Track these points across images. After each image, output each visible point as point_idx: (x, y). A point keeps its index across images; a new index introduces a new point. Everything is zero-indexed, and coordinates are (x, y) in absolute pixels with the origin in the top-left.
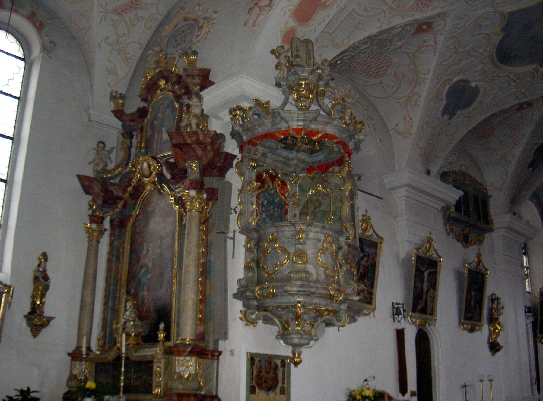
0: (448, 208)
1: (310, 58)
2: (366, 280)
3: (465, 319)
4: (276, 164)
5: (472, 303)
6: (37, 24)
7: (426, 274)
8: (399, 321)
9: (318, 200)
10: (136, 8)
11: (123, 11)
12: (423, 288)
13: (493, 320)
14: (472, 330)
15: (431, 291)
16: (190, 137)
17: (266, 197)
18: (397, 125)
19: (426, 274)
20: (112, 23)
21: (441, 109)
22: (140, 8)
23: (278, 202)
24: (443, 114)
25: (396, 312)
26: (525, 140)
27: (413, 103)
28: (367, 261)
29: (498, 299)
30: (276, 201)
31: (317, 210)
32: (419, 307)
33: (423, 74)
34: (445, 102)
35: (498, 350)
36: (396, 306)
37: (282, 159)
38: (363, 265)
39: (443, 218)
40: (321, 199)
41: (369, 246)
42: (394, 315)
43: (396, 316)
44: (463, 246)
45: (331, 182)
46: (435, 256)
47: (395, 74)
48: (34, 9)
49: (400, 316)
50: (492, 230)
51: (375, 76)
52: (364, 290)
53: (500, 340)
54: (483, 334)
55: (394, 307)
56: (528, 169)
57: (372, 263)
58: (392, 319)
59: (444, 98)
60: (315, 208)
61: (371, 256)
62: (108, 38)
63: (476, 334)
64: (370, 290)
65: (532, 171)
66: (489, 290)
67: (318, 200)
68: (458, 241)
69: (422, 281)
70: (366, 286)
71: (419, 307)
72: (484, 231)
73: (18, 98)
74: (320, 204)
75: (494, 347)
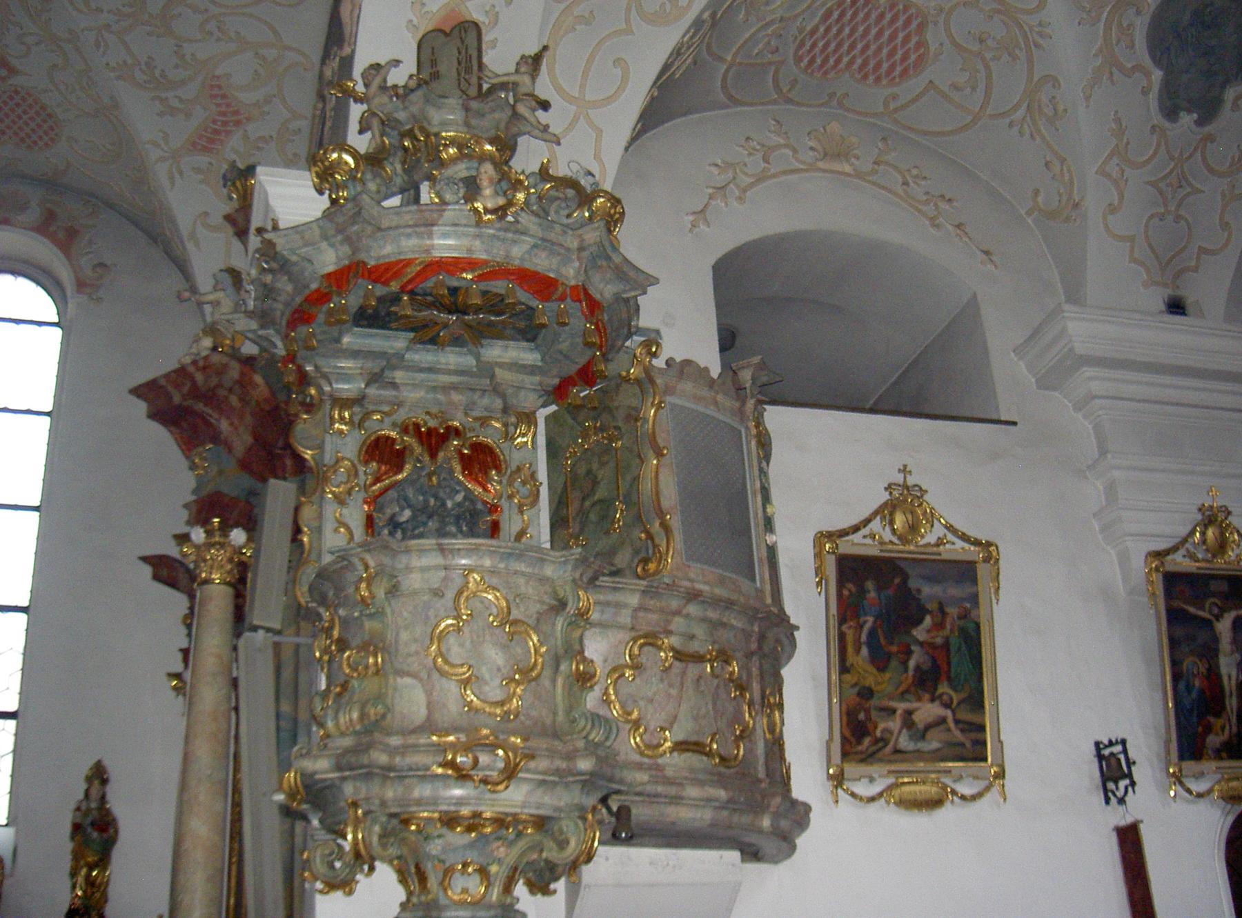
1: (468, 70)
2: (944, 688)
4: (440, 397)
6: (61, 235)
7: (1224, 627)
8: (1122, 801)
9: (589, 472)
10: (238, 123)
11: (212, 141)
12: (1219, 677)
16: (177, 387)
17: (406, 499)
18: (1037, 192)
19: (1224, 627)
20: (201, 177)
21: (1153, 97)
22: (248, 119)
23: (459, 505)
24: (1171, 113)
25: (1113, 769)
27: (1048, 111)
28: (939, 626)
30: (449, 504)
31: (587, 504)
33: (1029, 12)
34: (1157, 75)
36: (1106, 752)
37: (454, 379)
38: (921, 644)
40: (595, 466)
41: (932, 579)
42: (1105, 779)
43: (1111, 786)
45: (617, 408)
47: (954, 42)
48: (48, 205)
49: (1123, 784)
51: (905, 72)
52: (943, 720)
55: (1100, 757)
57: (964, 632)
59: (1147, 61)
60: (584, 499)
61: (953, 611)
62: (206, 214)
64: (965, 715)
67: (589, 472)
69: (1210, 652)
70: (947, 706)
71: (1214, 740)
73: (48, 414)
74: (595, 483)
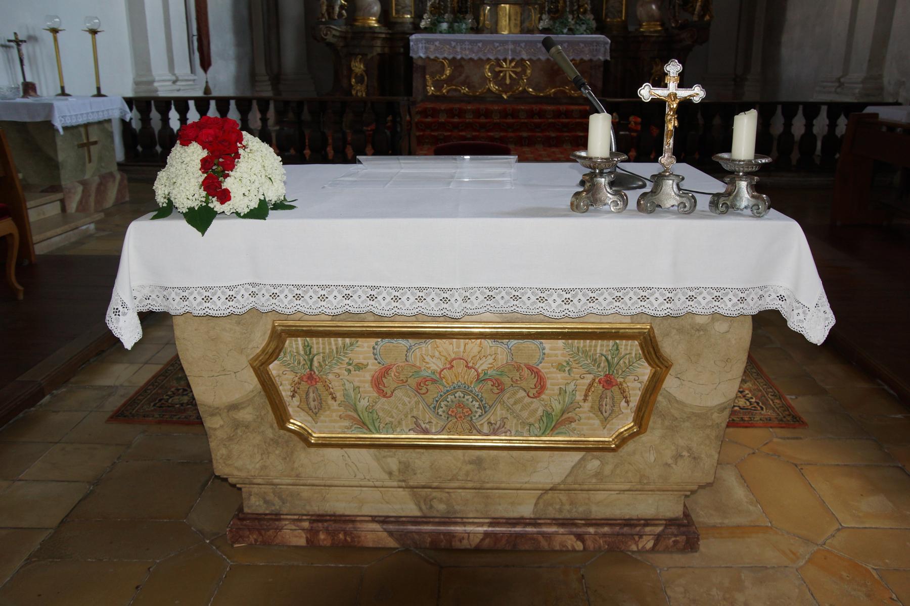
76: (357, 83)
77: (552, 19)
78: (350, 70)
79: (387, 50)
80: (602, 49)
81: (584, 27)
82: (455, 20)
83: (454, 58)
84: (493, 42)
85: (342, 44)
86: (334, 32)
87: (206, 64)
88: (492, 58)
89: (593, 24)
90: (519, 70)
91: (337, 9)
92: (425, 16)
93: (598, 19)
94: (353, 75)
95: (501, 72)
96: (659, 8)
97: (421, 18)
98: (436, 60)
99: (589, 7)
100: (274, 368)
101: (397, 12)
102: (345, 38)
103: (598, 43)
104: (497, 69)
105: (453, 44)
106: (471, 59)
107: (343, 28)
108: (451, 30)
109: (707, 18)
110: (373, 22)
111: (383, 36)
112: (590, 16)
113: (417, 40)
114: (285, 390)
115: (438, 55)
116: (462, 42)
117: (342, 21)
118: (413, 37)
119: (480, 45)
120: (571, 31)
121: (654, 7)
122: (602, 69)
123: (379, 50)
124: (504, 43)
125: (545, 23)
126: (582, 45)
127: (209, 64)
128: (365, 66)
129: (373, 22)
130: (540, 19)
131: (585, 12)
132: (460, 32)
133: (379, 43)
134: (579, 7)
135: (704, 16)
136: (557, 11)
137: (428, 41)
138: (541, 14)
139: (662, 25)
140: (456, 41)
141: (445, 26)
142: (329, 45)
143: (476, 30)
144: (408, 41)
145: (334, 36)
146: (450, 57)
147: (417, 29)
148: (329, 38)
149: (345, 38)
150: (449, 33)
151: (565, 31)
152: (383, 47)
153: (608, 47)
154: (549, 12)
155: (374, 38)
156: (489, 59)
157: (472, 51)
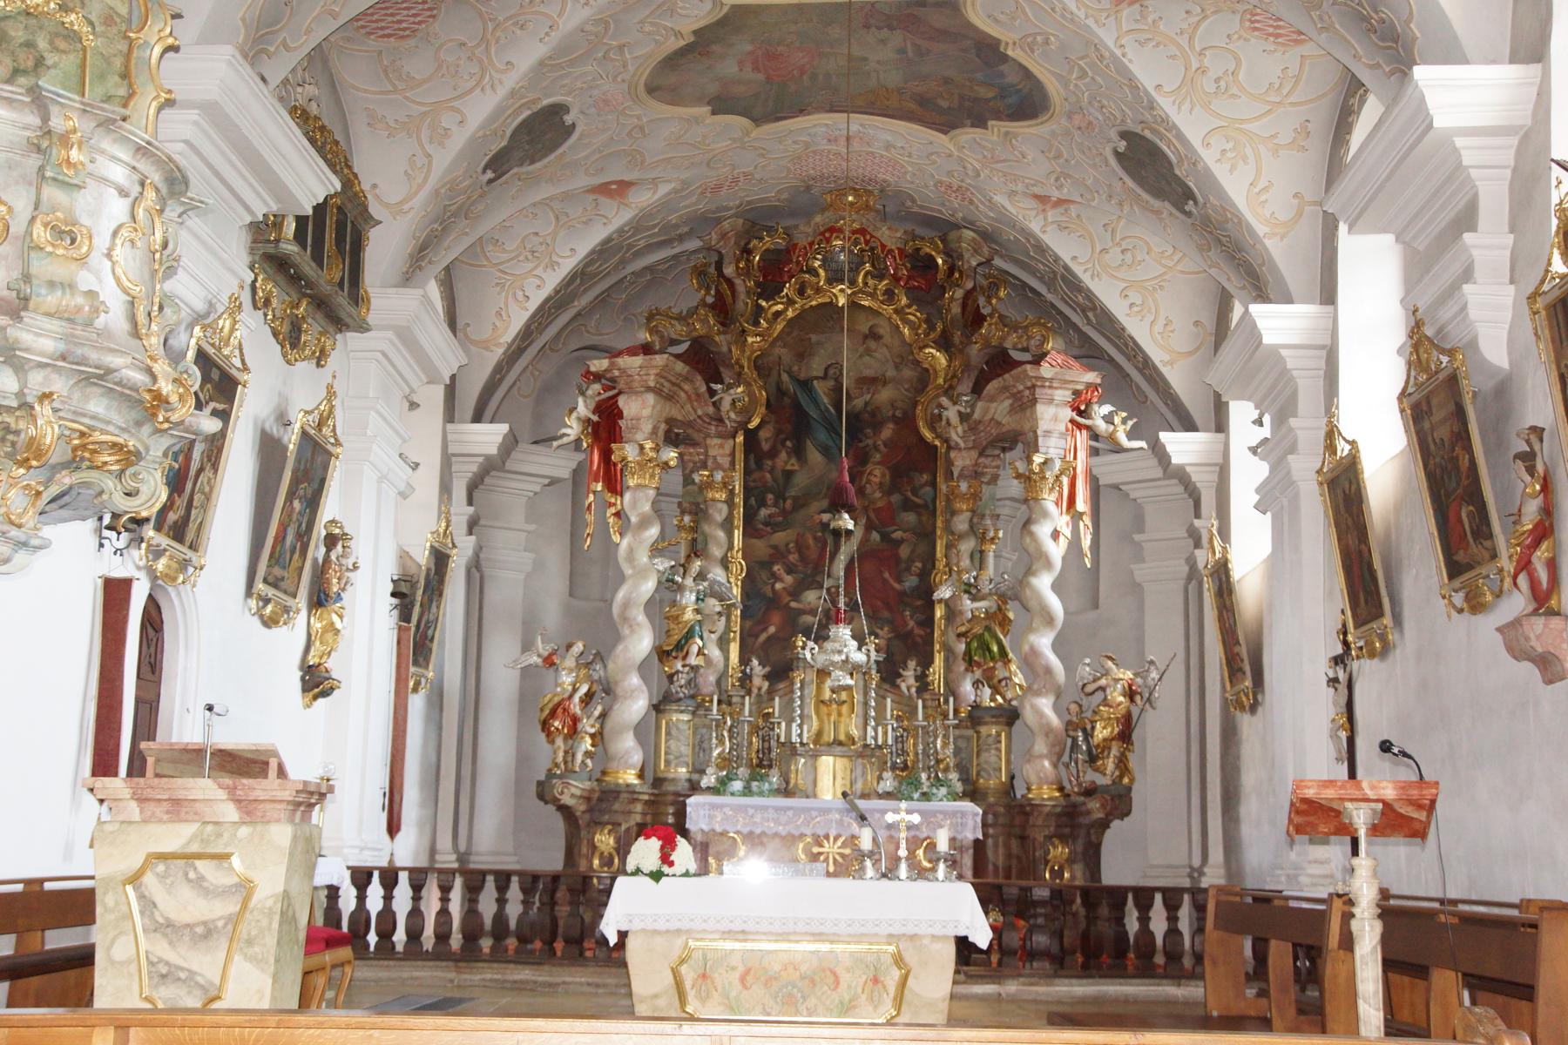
0: (277, 222)
3: (265, 581)
5: (290, 539)
13: (320, 599)
14: (269, 622)
15: (208, 473)
26: (511, 81)
29: (345, 537)
32: (172, 517)
35: (325, 694)
39: (252, 251)
44: (284, 355)
46: (237, 362)
50: (363, 327)
53: (334, 665)
54: (290, 639)
56: (484, 172)
58: (95, 542)
63: (279, 632)
65: (490, 181)
66: (331, 508)
68: (275, 334)
72: (338, 323)
75: (316, 682)
76: (602, 865)
77: (900, 780)
78: (593, 847)
79: (649, 819)
80: (971, 823)
81: (943, 791)
82: (753, 778)
83: (751, 833)
84: (810, 809)
85: (583, 808)
86: (573, 790)
87: (393, 828)
88: (808, 832)
89: (959, 787)
90: (847, 851)
91: (579, 757)
92: (709, 770)
93: (965, 779)
94: (597, 855)
95: (820, 854)
96: (1055, 766)
97: (702, 772)
98: (724, 834)
99: (951, 762)
100: (684, 969)
101: (668, 763)
102: (588, 799)
103: (963, 814)
104: (816, 850)
105: (751, 811)
106: (776, 835)
107: (587, 785)
108: (747, 791)
109: (1126, 780)
110: (630, 777)
111: (646, 797)
112: (954, 776)
113: (697, 805)
114: (688, 984)
115: (728, 828)
116: (764, 808)
117: (585, 775)
118: (690, 801)
119: (790, 813)
120: (926, 796)
121: (1047, 763)
122: (971, 851)
123: (638, 818)
124: (825, 811)
125: (888, 783)
126: (940, 817)
127: (398, 829)
128: (618, 841)
129: (630, 777)
130: (880, 778)
131: (946, 770)
132: (761, 794)
133: (639, 807)
134: (938, 762)
135: (1121, 777)
136: (905, 767)
137: (713, 807)
138: (882, 769)
139: (1061, 789)
140: (755, 807)
141: (737, 785)
142: (565, 810)
143: (786, 791)
144: (684, 805)
145: (573, 795)
146: (745, 830)
147: (694, 788)
148: (567, 800)
149: (588, 799)
150: (745, 795)
151: (916, 796)
152: (644, 814)
153: (979, 819)
154: (894, 768)
155: (634, 801)
156: (802, 836)
157: (777, 822)
